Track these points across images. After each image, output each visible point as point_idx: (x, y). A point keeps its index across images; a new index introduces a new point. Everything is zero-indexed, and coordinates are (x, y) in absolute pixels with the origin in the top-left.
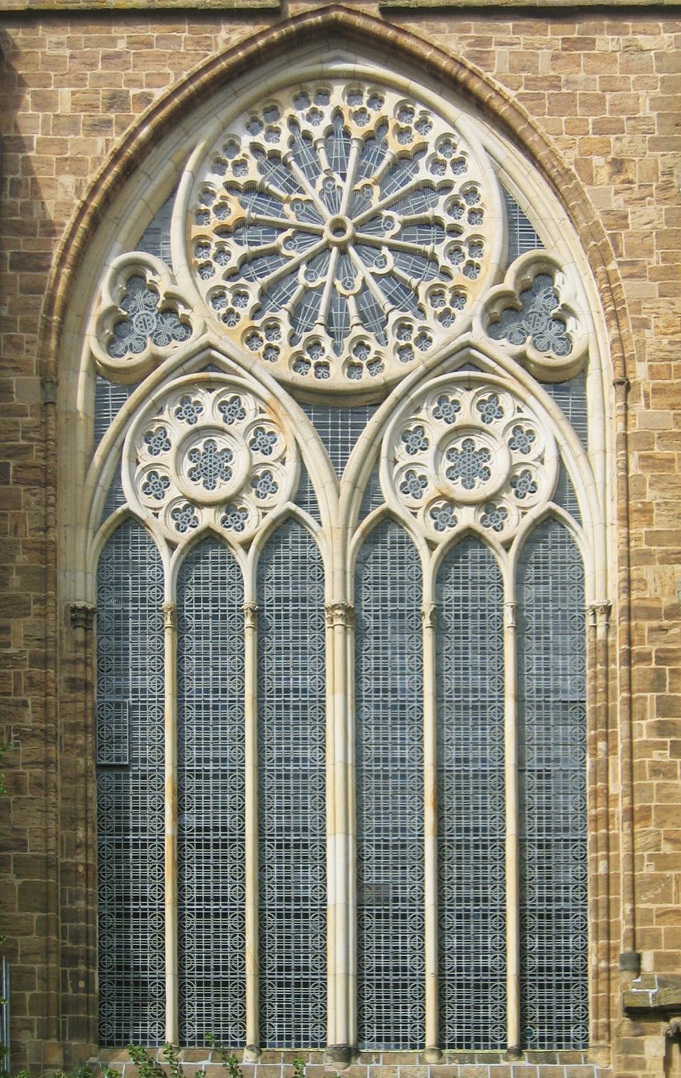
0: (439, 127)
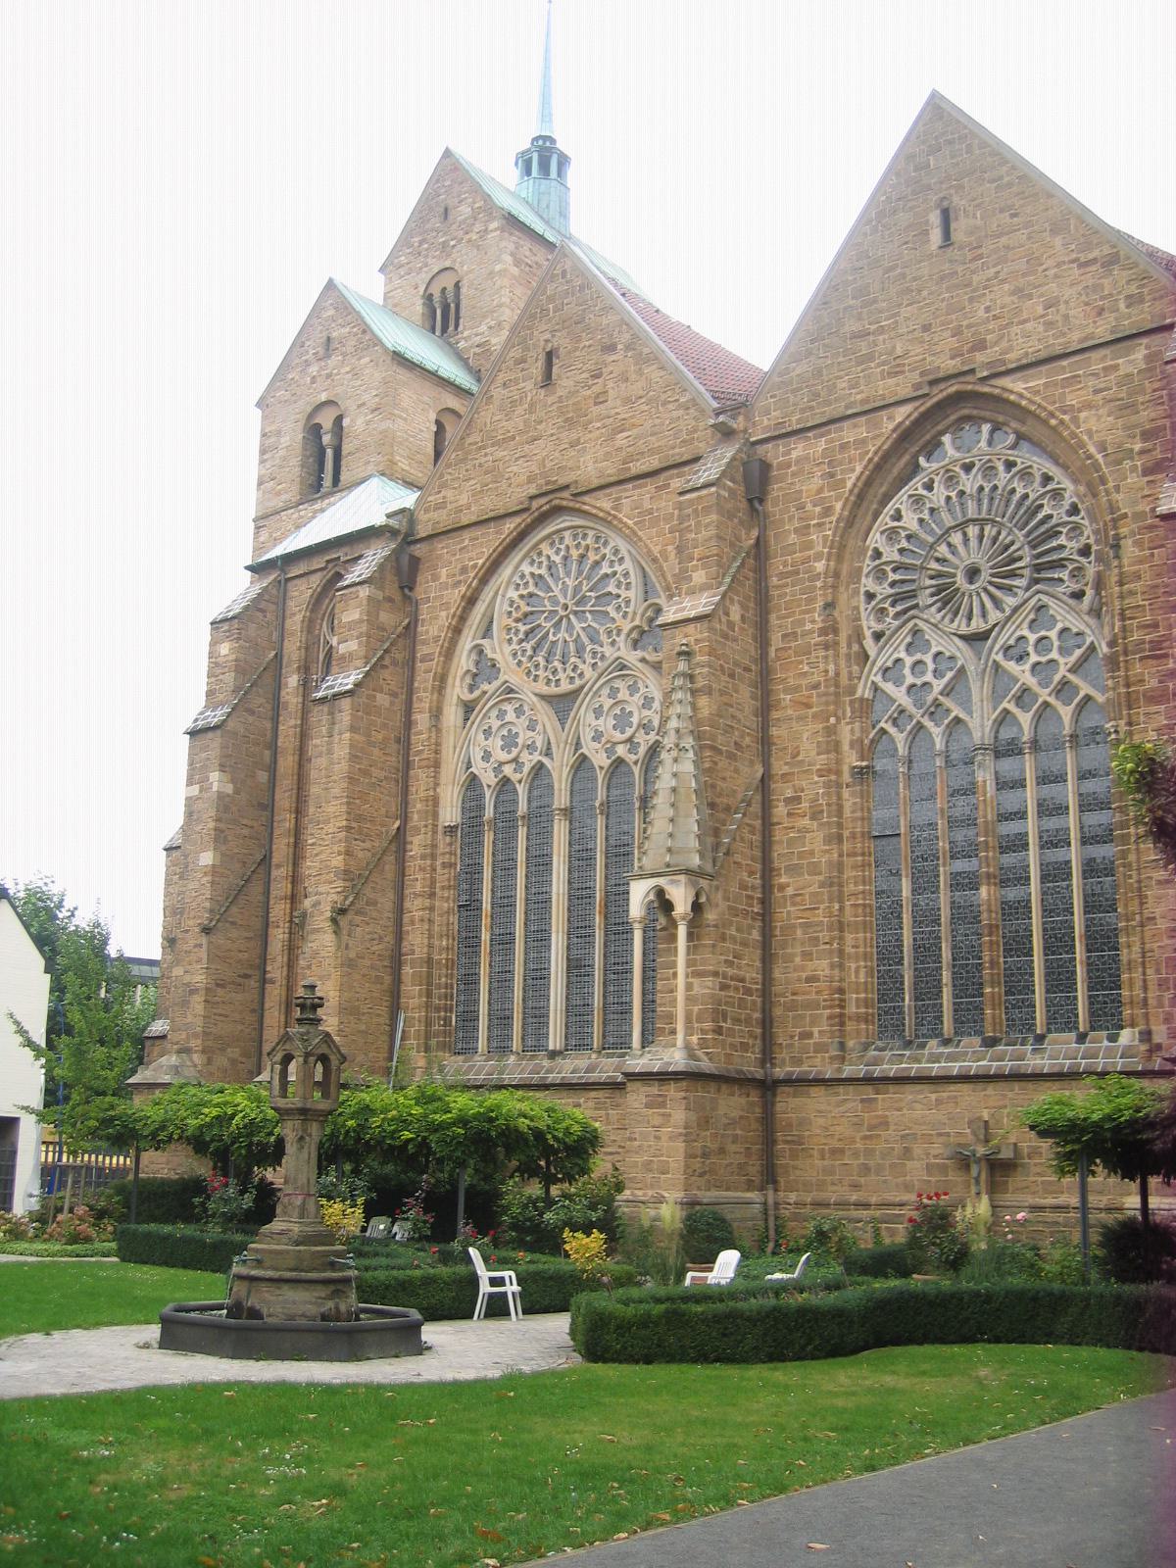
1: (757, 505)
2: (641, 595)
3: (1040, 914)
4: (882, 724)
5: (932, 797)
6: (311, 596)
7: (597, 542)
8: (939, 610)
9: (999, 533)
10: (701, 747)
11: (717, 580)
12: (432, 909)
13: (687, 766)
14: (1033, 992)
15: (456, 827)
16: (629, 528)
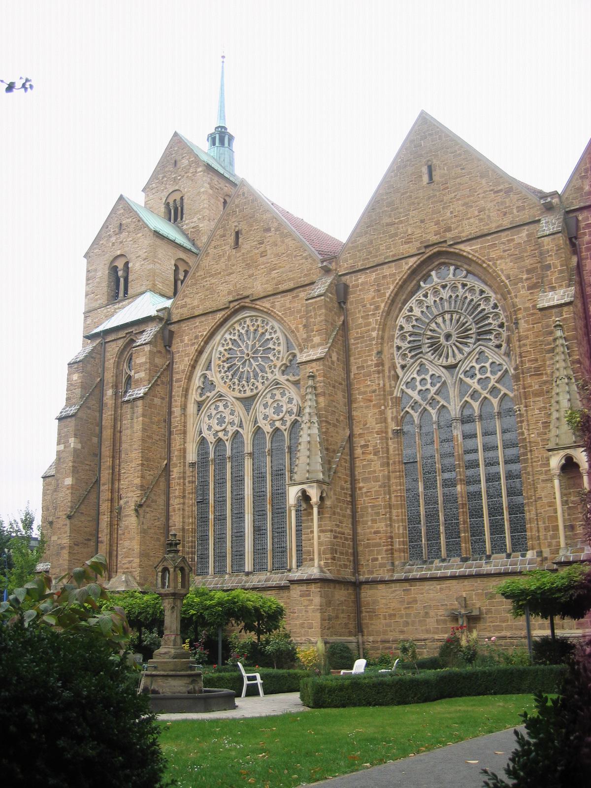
0: (270, 324)
1: (342, 305)
2: (286, 349)
3: (486, 497)
4: (407, 409)
5: (432, 442)
6: (118, 351)
7: (262, 323)
8: (432, 354)
9: (460, 318)
10: (321, 421)
11: (326, 340)
12: (184, 504)
13: (315, 431)
14: (484, 535)
15: (195, 463)
16: (279, 316)
